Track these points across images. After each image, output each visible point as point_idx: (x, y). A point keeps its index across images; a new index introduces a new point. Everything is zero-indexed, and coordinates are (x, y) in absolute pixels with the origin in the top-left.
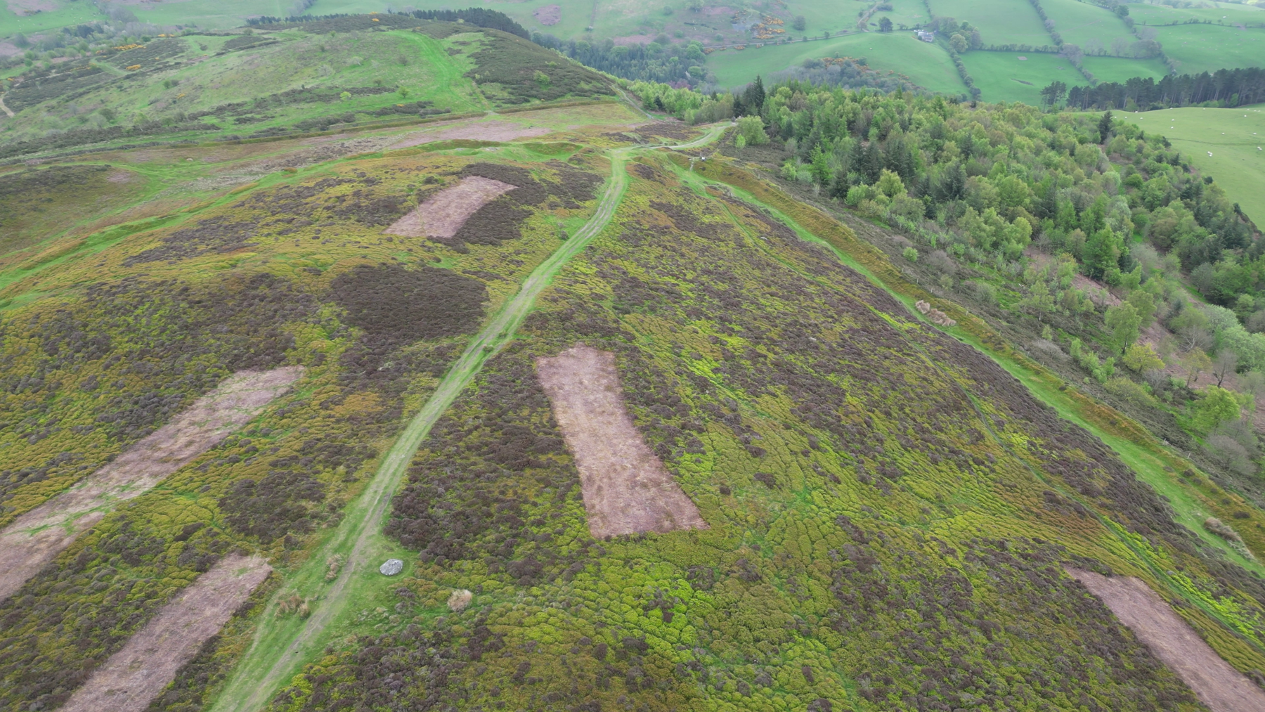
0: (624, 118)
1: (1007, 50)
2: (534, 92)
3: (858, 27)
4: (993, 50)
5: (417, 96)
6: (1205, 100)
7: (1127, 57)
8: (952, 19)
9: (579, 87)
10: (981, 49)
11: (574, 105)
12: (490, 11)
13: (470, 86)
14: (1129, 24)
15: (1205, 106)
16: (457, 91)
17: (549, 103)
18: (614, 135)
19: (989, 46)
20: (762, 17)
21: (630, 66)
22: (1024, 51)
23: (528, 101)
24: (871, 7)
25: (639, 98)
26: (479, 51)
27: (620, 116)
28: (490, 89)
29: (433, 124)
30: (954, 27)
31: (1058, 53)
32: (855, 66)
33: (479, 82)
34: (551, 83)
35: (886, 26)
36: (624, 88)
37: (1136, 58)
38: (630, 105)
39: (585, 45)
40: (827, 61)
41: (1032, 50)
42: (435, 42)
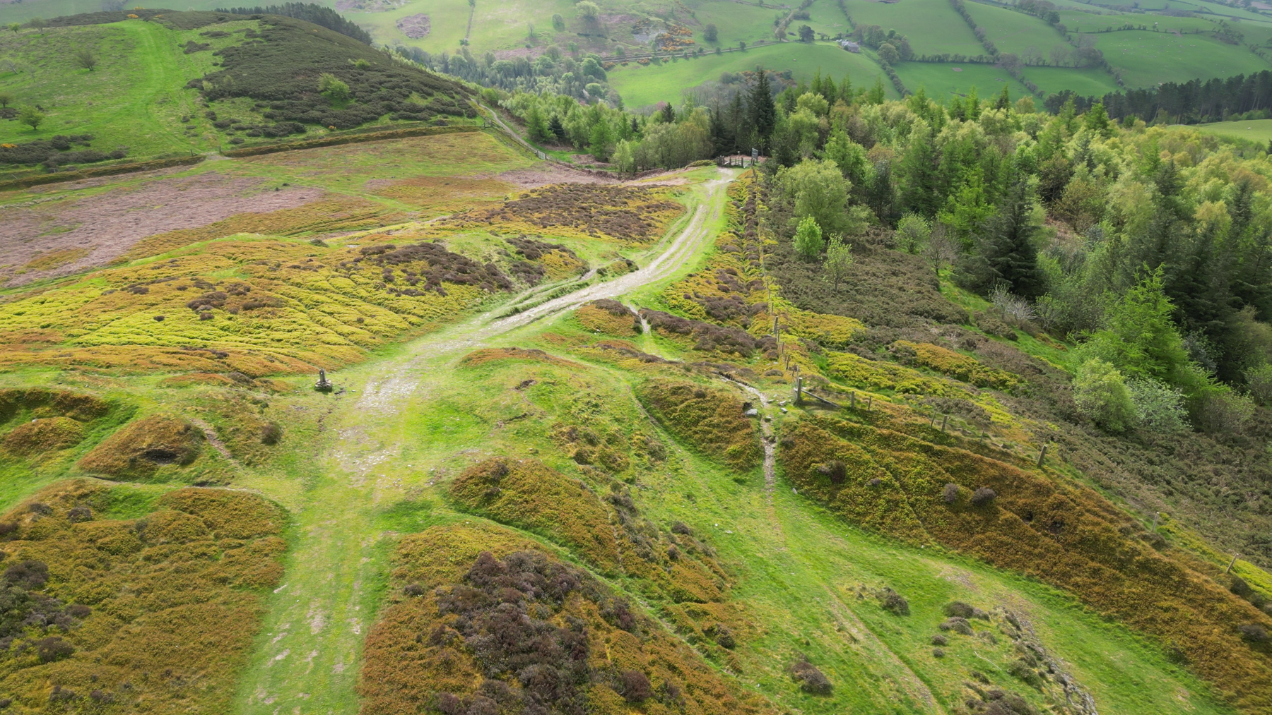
0: (493, 160)
1: (940, 60)
2: (315, 113)
3: (776, 37)
4: (924, 61)
5: (55, 123)
6: (1248, 110)
7: (1066, 67)
8: (878, 27)
9: (407, 102)
10: (911, 60)
11: (393, 136)
12: (312, 5)
13: (191, 103)
14: (1062, 31)
15: (1249, 118)
16: (160, 114)
17: (347, 134)
18: (408, 256)
19: (921, 57)
20: (668, 27)
21: (516, 84)
22: (957, 62)
23: (302, 131)
24: (786, 15)
25: (520, 121)
26: (238, 45)
27: (484, 157)
28: (223, 109)
29: (66, 185)
30: (880, 36)
31: (993, 64)
32: (779, 80)
33: (212, 96)
34: (353, 95)
35: (807, 35)
36: (493, 103)
37: (1077, 68)
38: (504, 134)
39: (460, 60)
40: (746, 74)
41: (966, 60)
42: (169, 32)
